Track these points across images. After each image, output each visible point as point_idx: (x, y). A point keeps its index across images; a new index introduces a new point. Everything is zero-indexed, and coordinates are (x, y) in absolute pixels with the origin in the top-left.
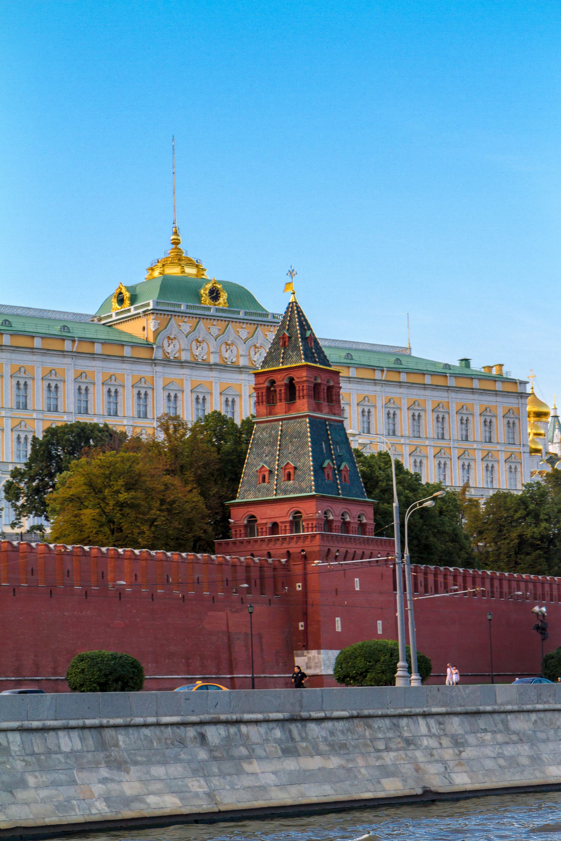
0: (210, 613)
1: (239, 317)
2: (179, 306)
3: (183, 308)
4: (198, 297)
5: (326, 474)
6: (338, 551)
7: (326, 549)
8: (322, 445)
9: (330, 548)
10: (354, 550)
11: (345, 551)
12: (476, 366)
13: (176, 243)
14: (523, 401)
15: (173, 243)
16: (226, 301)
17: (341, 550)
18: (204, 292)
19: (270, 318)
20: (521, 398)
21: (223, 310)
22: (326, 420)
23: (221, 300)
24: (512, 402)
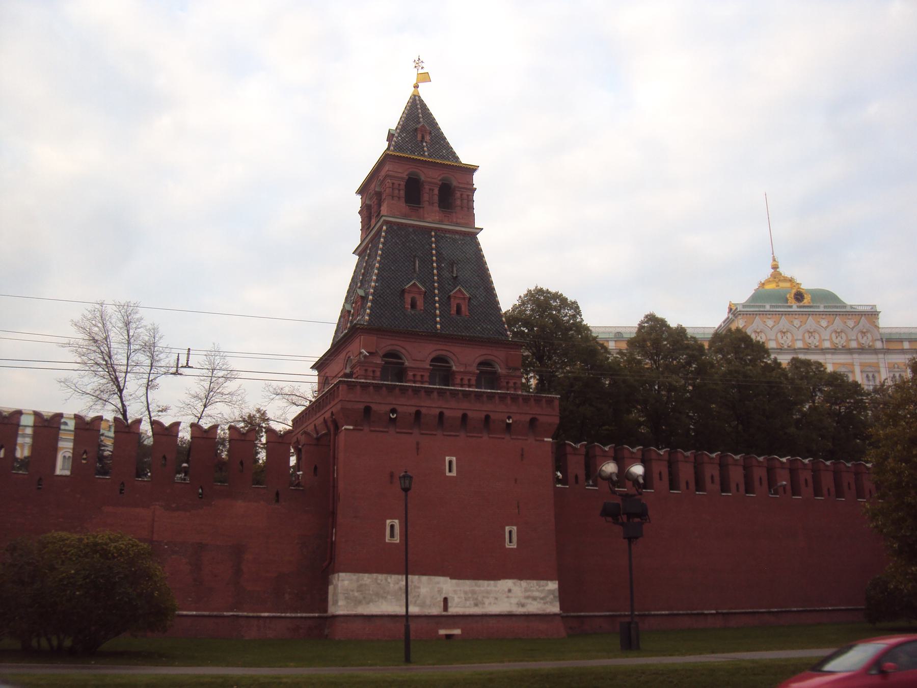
2: (764, 307)
3: (768, 308)
4: (786, 300)
6: (393, 411)
7: (362, 406)
9: (372, 406)
10: (438, 411)
13: (775, 267)
15: (773, 268)
16: (809, 301)
17: (399, 409)
18: (790, 296)
19: (848, 309)
21: (804, 307)
22: (432, 229)
23: (805, 301)
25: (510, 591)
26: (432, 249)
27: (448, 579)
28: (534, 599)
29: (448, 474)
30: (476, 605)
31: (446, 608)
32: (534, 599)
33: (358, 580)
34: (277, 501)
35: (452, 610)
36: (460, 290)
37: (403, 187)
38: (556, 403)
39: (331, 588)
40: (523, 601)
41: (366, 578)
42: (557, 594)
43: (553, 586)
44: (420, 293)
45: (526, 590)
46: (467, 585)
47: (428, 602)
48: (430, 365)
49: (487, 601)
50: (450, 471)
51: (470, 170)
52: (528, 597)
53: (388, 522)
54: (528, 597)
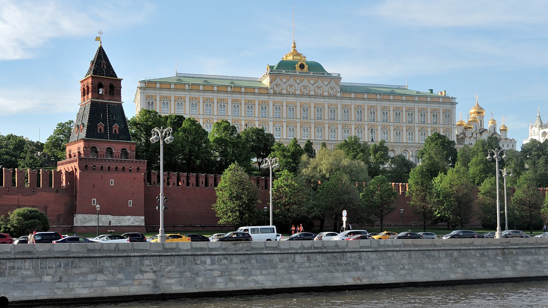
0: (4, 196)
1: (310, 75)
2: (282, 71)
5: (99, 129)
6: (94, 166)
7: (85, 165)
8: (101, 115)
10: (108, 166)
11: (115, 167)
12: (436, 92)
14: (454, 106)
20: (452, 105)
23: (305, 68)
24: (448, 107)
25: (129, 219)
26: (107, 110)
27: (111, 216)
28: (137, 221)
29: (111, 185)
30: (119, 223)
31: (110, 224)
32: (137, 221)
33: (84, 216)
34: (57, 192)
35: (112, 225)
36: (116, 125)
37: (96, 87)
38: (146, 163)
39: (75, 218)
40: (134, 222)
41: (86, 216)
42: (144, 220)
43: (143, 218)
44: (103, 126)
45: (134, 219)
46: (116, 217)
47: (105, 223)
48: (106, 151)
49: (122, 222)
50: (112, 184)
51: (120, 80)
52: (134, 221)
53: (93, 199)
54: (135, 221)
